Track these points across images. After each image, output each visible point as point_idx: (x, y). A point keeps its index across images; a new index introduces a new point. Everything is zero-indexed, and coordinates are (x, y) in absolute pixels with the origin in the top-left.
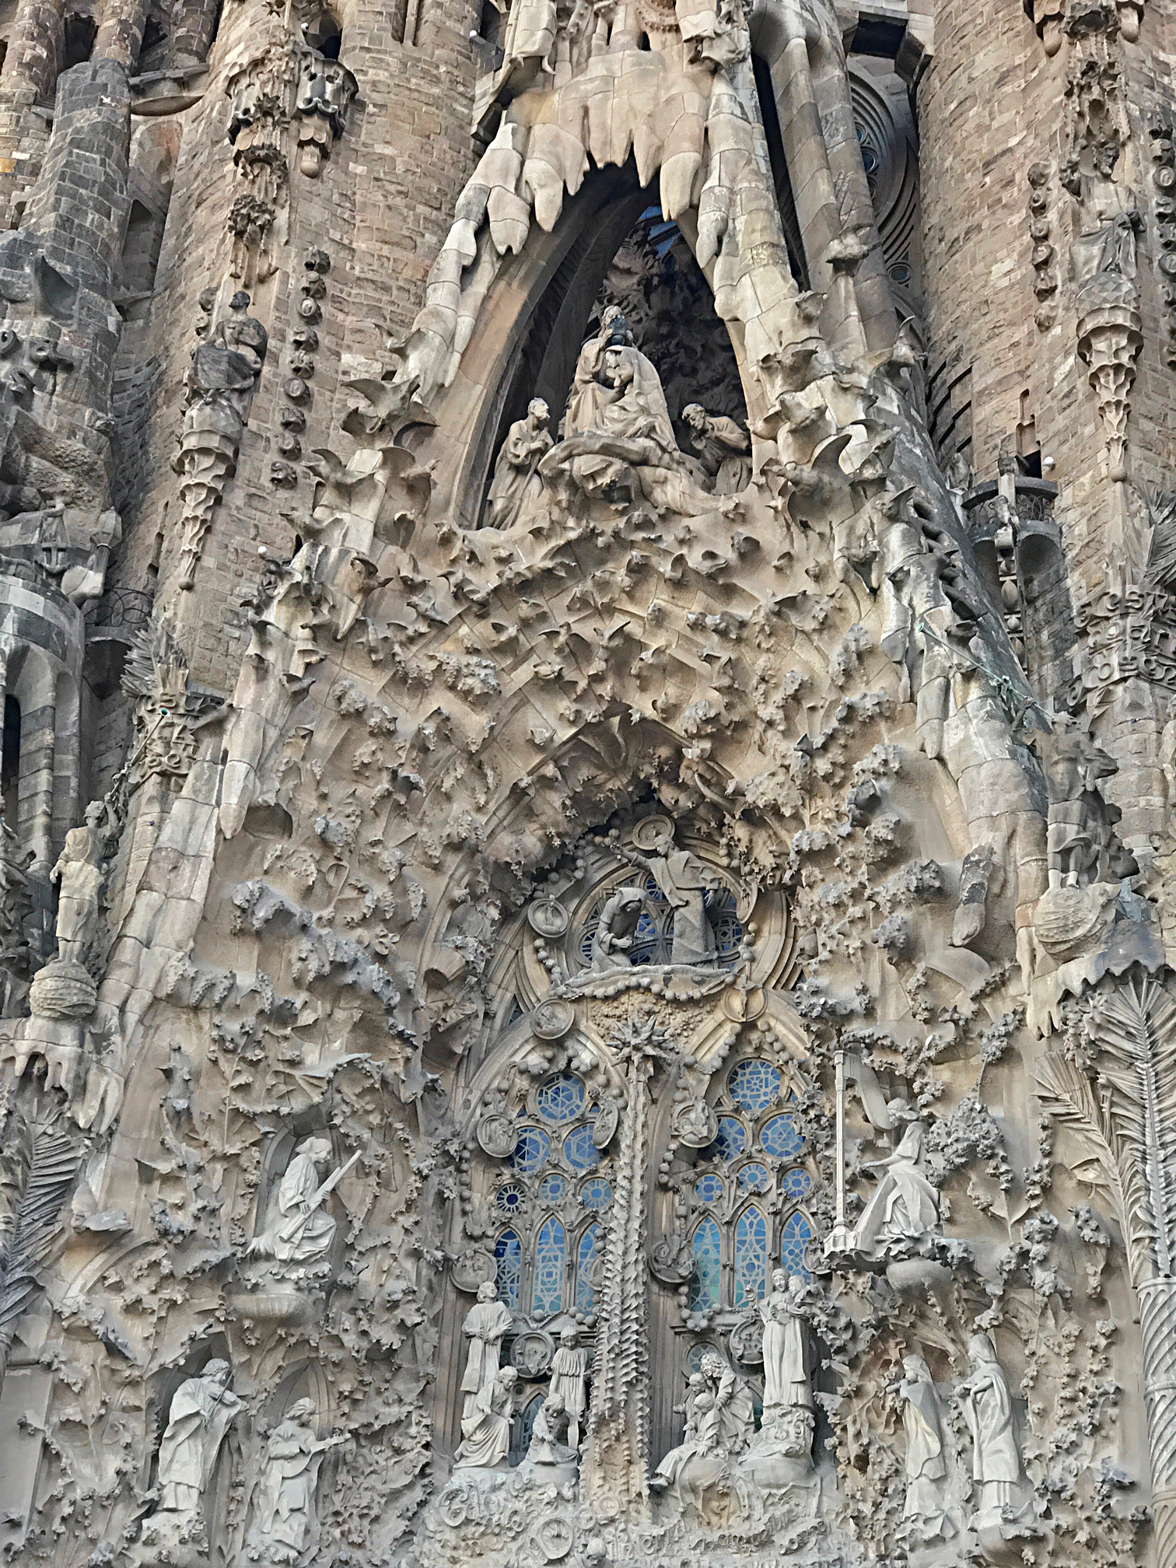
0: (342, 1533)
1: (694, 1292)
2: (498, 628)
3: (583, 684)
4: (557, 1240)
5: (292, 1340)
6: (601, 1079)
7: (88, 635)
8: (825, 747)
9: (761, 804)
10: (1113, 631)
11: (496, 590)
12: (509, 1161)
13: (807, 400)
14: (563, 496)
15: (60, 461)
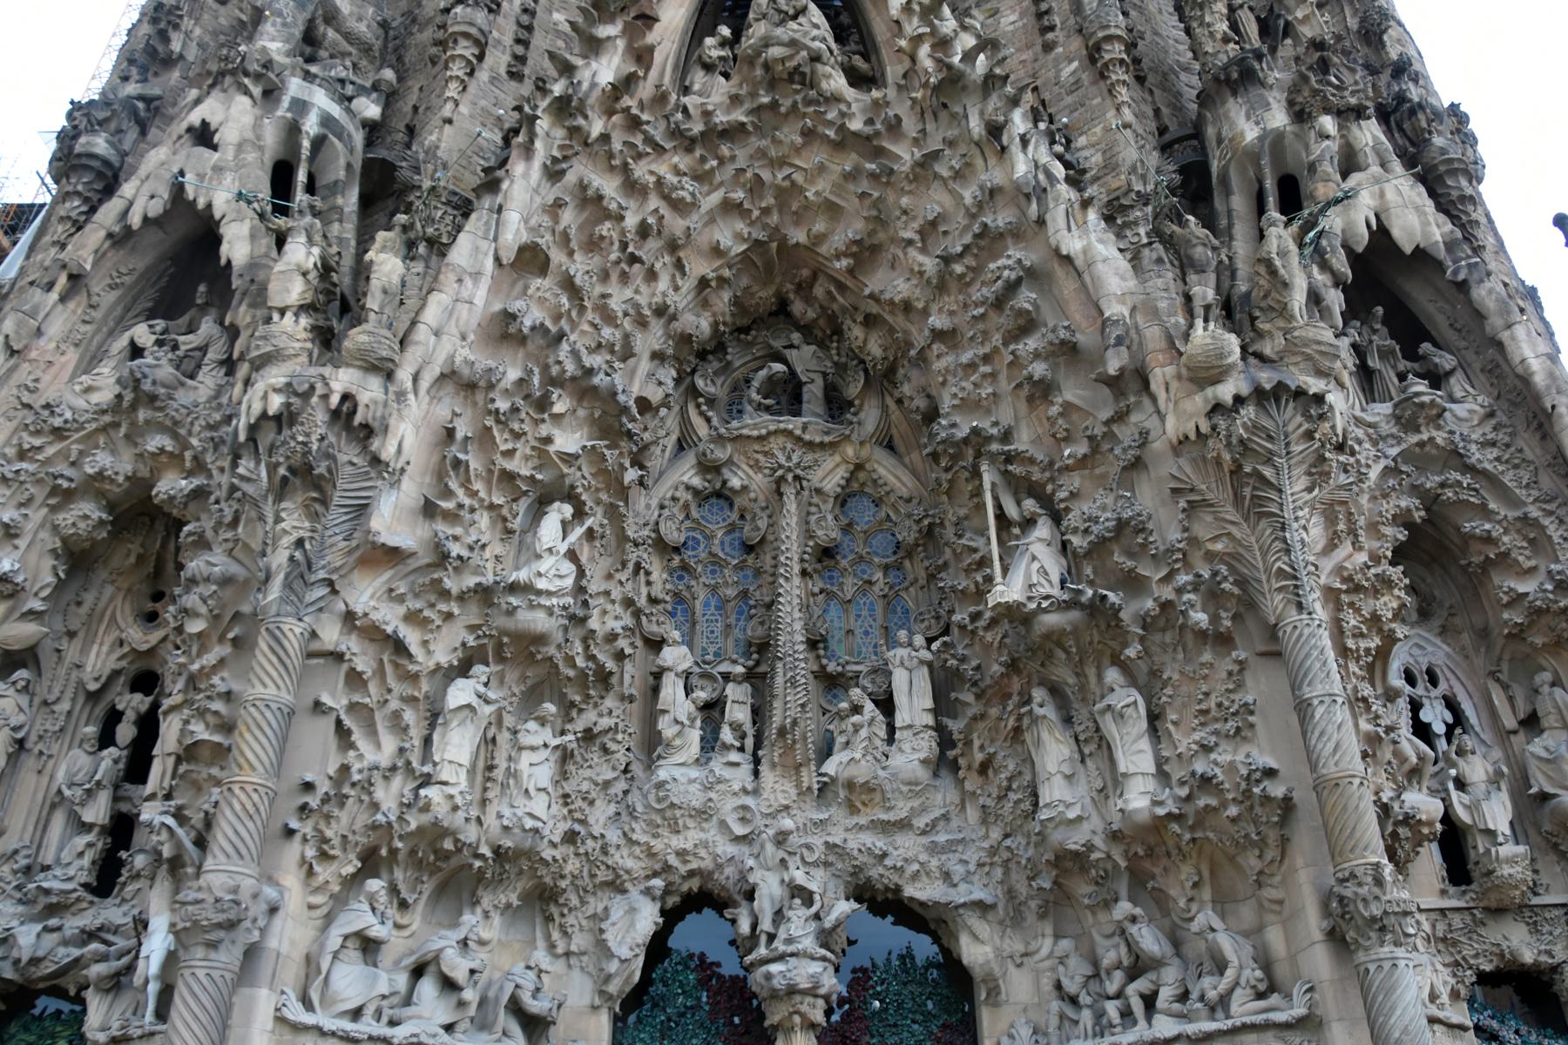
0: (570, 812)
1: (825, 649)
2: (703, 159)
3: (756, 213)
4: (717, 608)
5: (539, 657)
6: (752, 495)
7: (365, 152)
8: (961, 255)
9: (897, 299)
10: (1138, 214)
11: (702, 134)
12: (677, 550)
13: (948, 24)
14: (759, 72)
15: (348, 36)
